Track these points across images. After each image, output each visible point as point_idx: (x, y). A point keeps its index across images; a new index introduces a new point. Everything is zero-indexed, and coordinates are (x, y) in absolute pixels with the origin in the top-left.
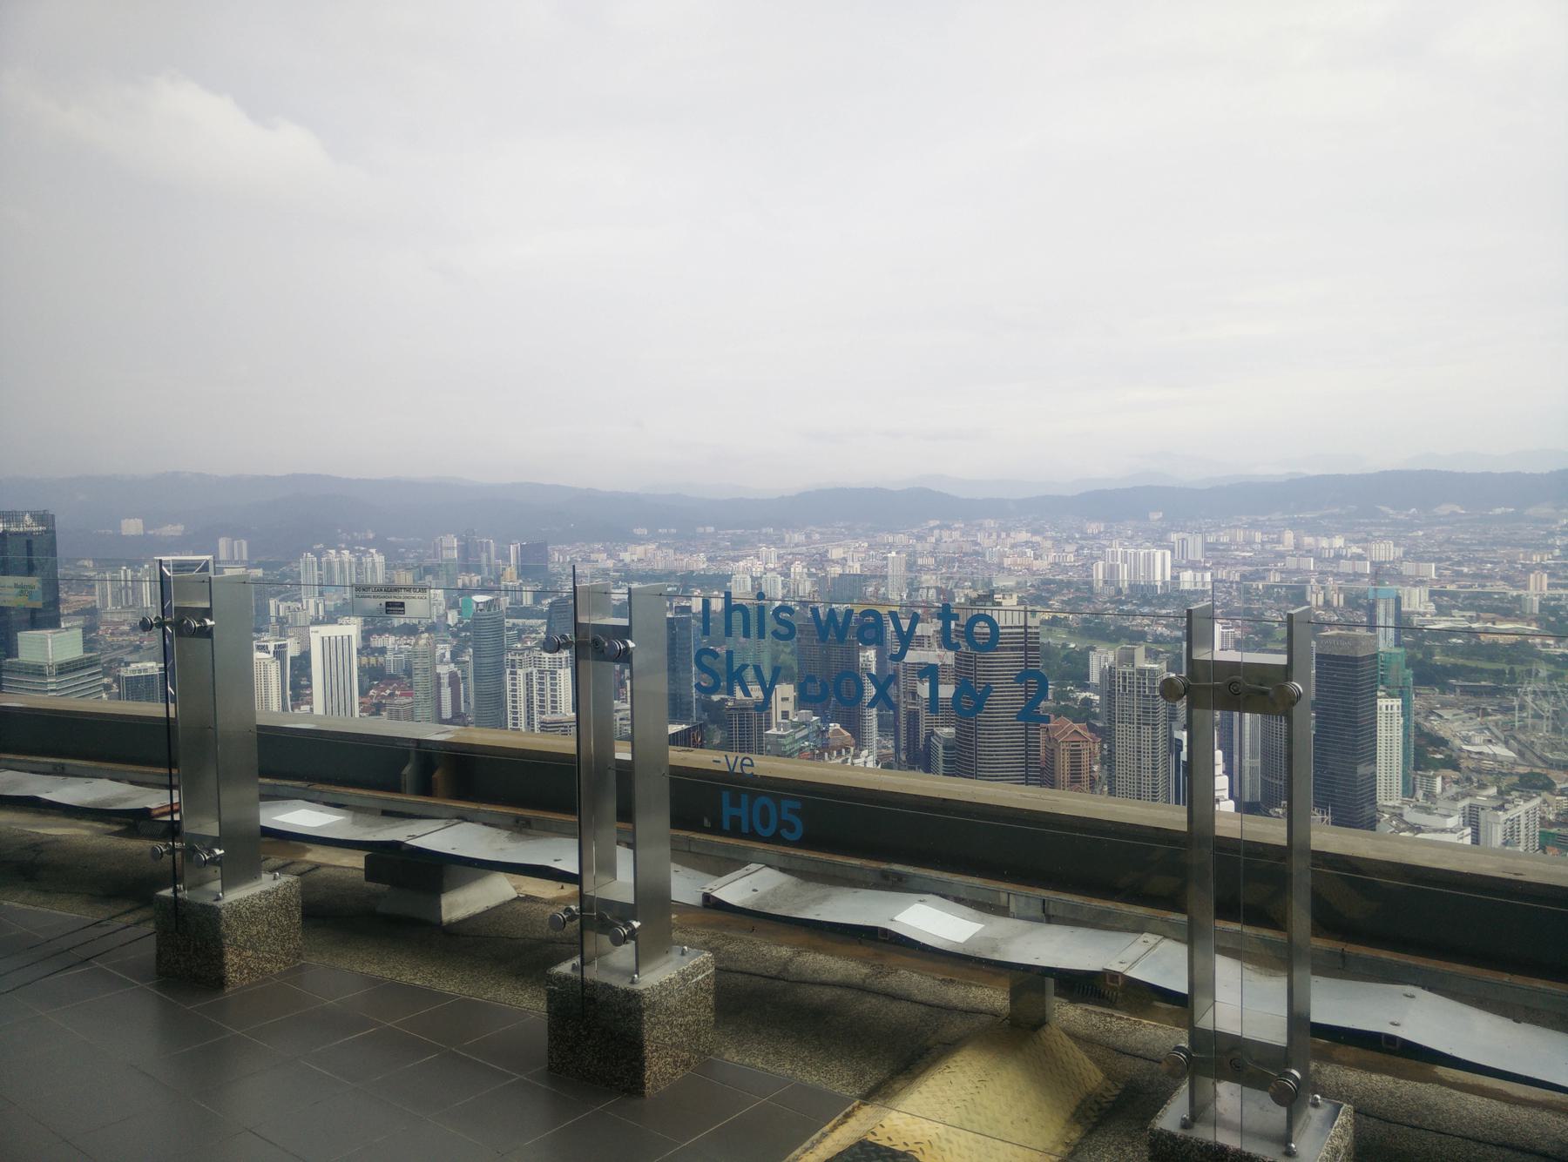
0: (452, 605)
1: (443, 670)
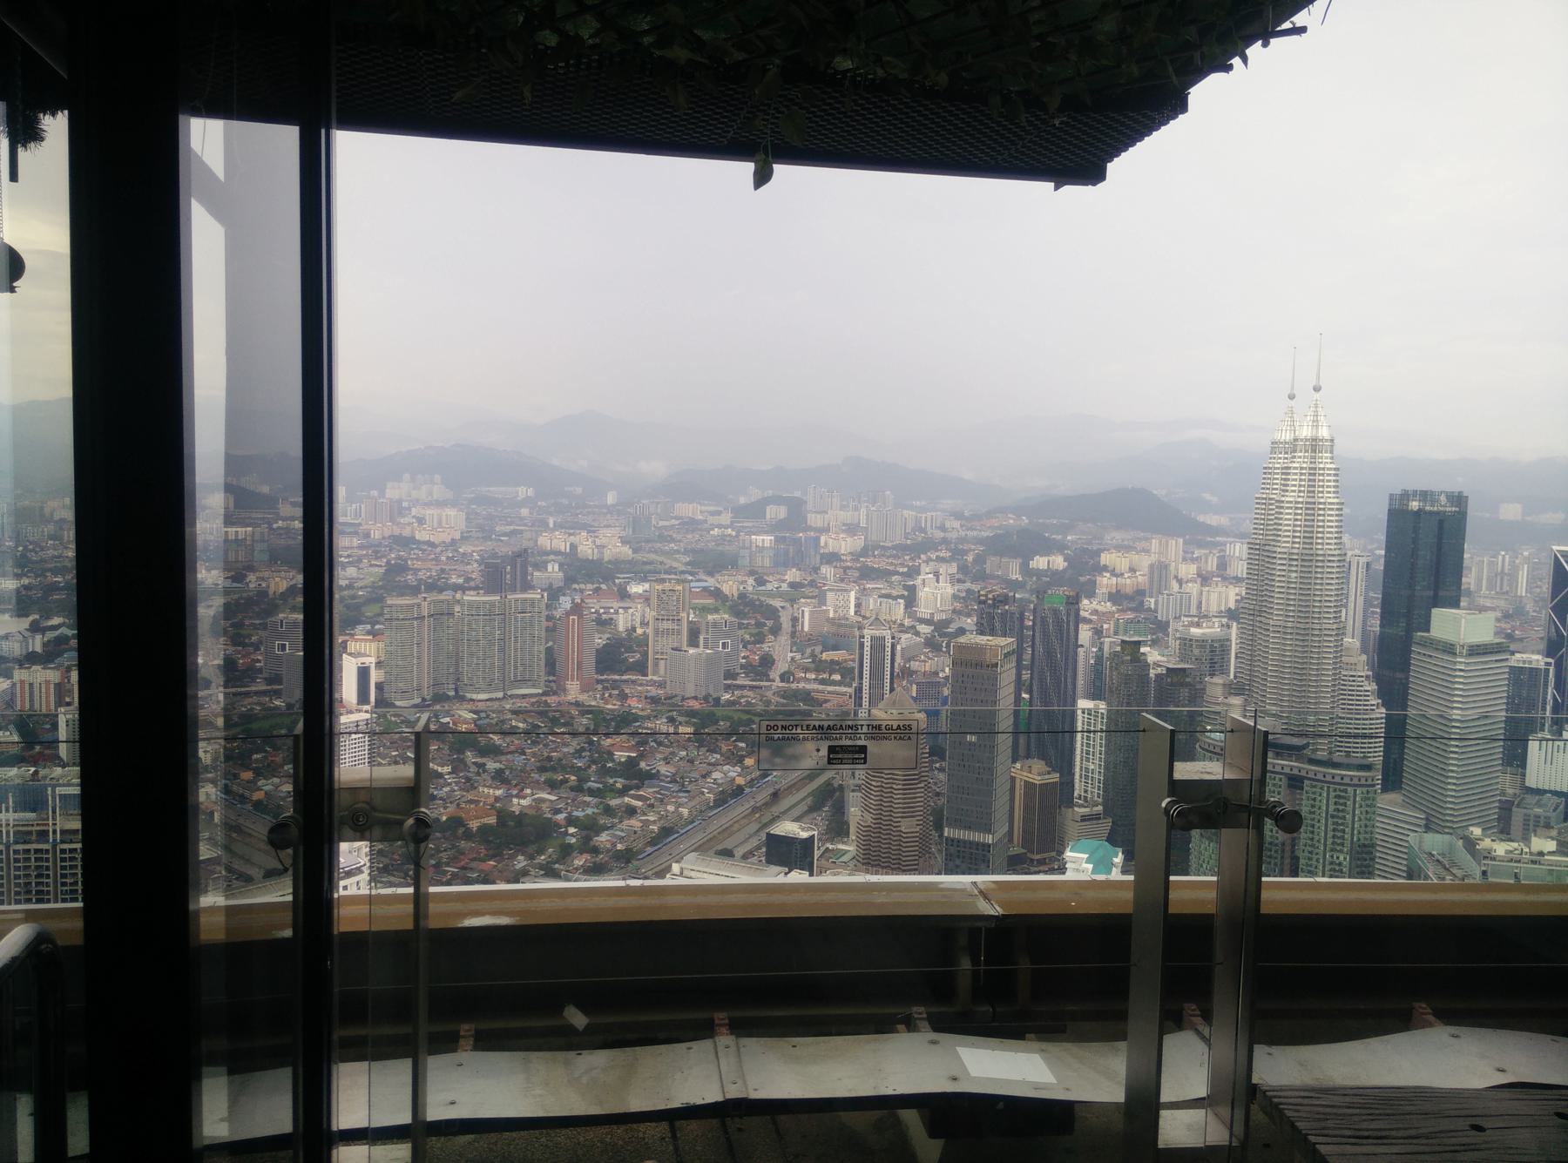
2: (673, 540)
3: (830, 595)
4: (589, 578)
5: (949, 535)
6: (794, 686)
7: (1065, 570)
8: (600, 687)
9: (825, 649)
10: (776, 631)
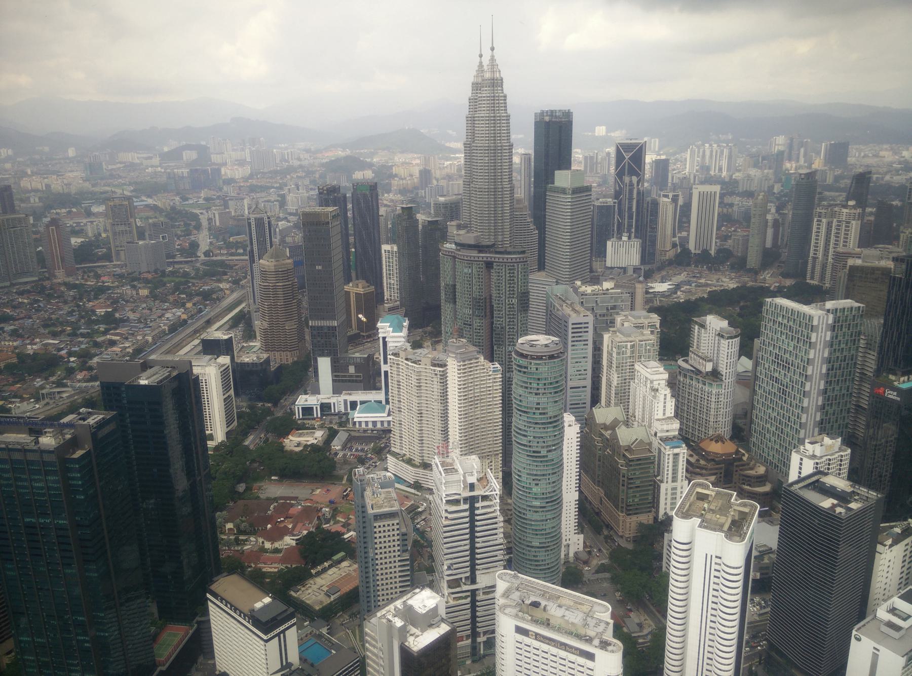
0: (779, 180)
1: (769, 217)
2: (120, 177)
3: (230, 202)
4: (63, 205)
5: (303, 163)
6: (214, 258)
7: (374, 178)
8: (80, 272)
9: (232, 235)
10: (198, 227)
